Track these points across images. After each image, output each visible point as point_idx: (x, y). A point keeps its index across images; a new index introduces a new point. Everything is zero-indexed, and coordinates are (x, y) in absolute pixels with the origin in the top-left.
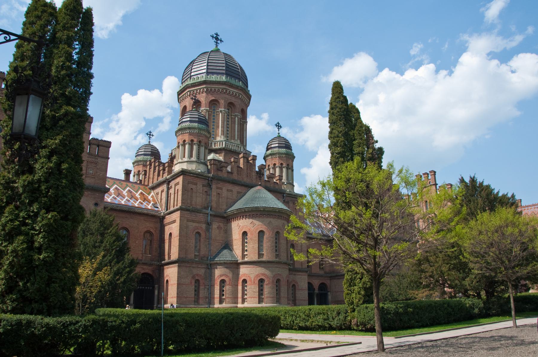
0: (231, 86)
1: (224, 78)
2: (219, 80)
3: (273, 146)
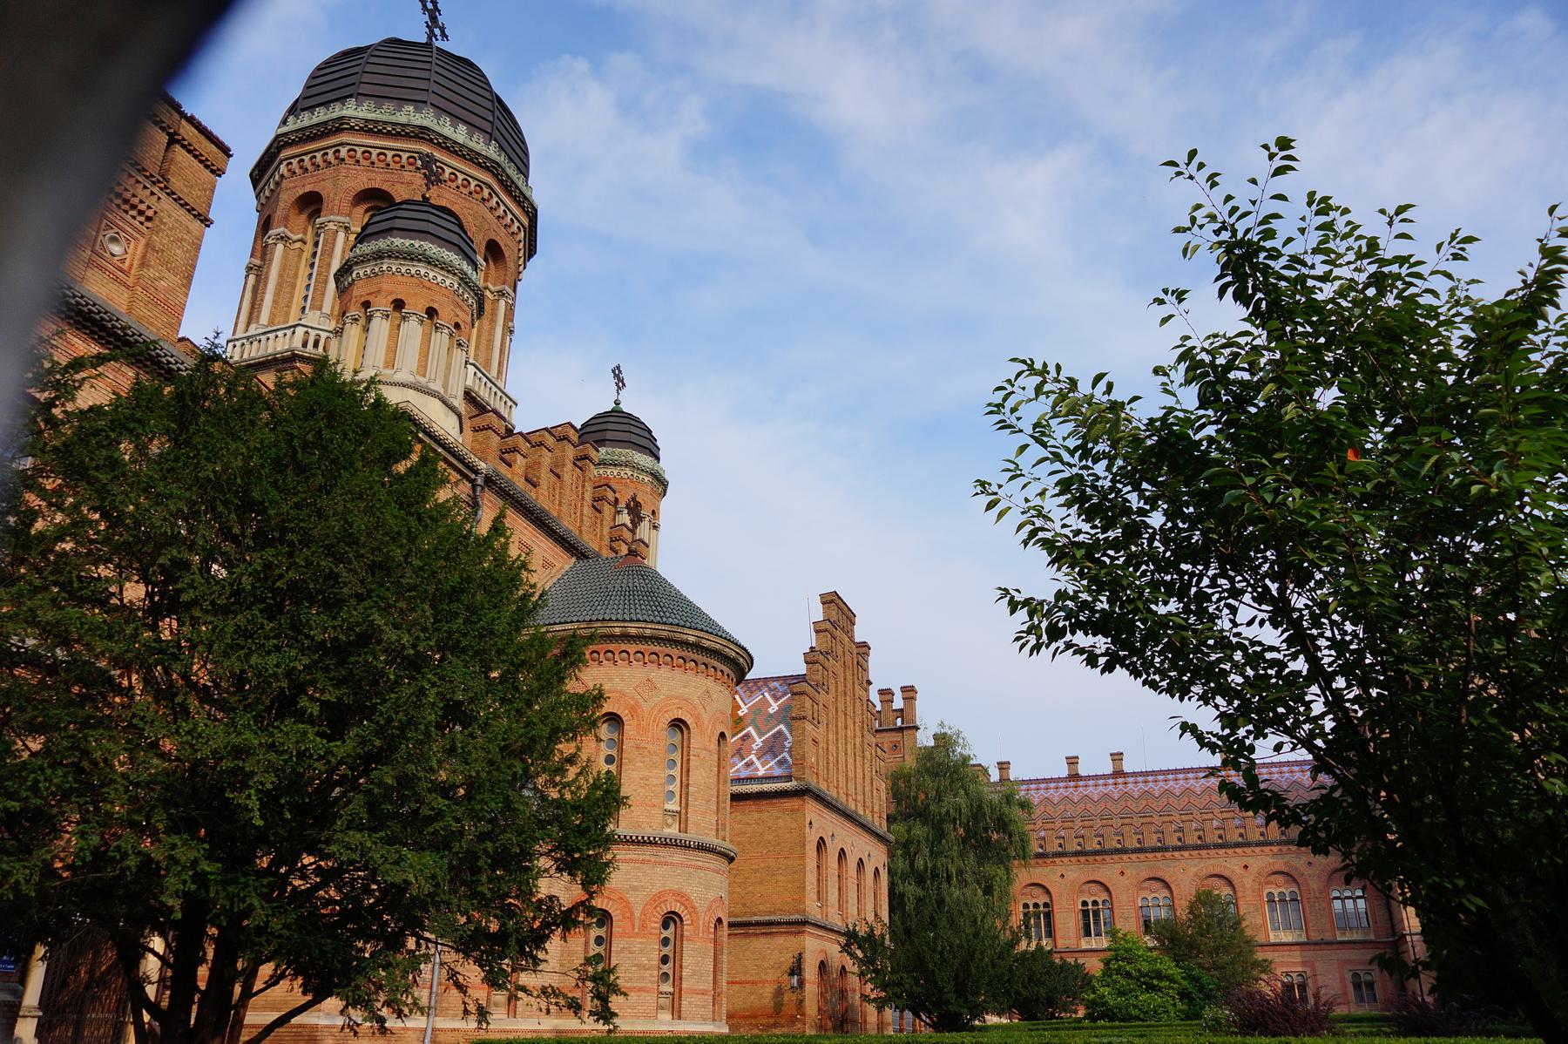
0: (509, 187)
1: (492, 151)
2: (472, 145)
3: (609, 435)
